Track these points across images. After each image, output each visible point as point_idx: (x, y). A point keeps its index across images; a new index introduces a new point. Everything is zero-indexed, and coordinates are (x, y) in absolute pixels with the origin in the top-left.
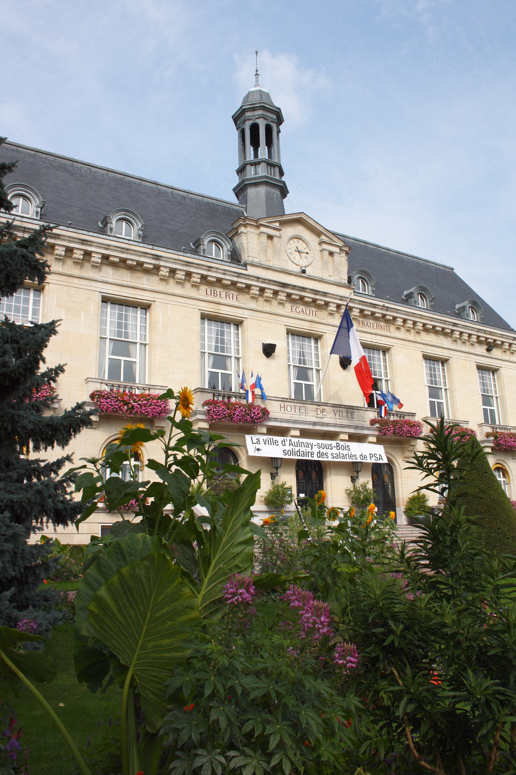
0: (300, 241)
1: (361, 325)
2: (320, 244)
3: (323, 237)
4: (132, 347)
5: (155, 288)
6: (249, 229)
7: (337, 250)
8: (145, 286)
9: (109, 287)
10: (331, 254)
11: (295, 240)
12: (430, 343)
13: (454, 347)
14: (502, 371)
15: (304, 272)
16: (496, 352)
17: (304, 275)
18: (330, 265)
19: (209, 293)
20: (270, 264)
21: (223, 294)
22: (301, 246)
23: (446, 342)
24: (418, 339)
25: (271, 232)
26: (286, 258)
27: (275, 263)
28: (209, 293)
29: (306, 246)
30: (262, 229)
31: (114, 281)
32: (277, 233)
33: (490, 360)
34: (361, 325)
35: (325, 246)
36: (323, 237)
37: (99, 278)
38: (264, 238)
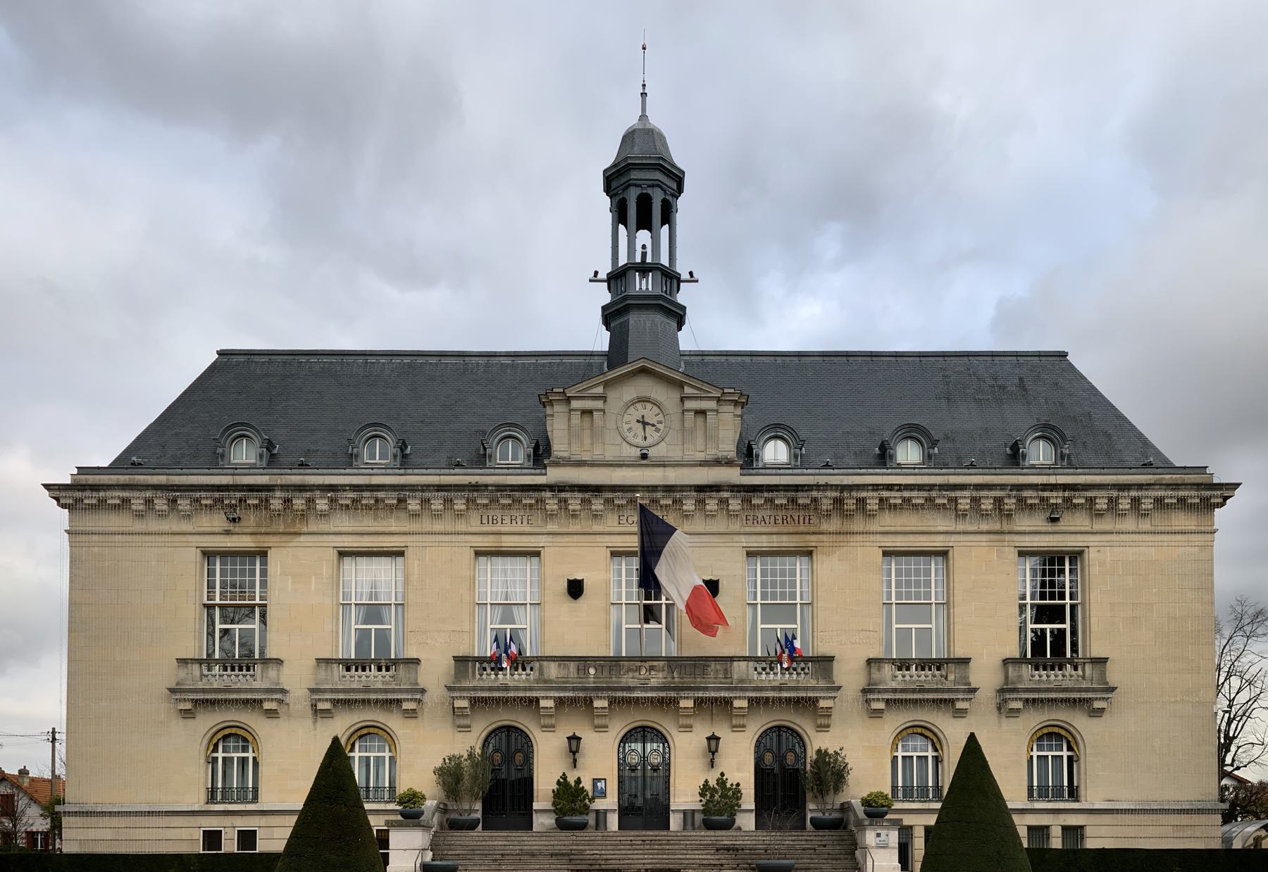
0: (649, 406)
1: (750, 523)
2: (682, 399)
3: (688, 390)
4: (384, 610)
5: (406, 529)
6: (558, 408)
7: (712, 404)
8: (393, 529)
9: (345, 538)
10: (702, 413)
11: (639, 406)
12: (899, 529)
13: (961, 527)
14: (1092, 556)
15: (644, 456)
17: (645, 462)
18: (700, 434)
19: (485, 521)
20: (586, 457)
21: (507, 520)
22: (650, 413)
23: (941, 522)
24: (874, 526)
27: (597, 453)
28: (485, 521)
29: (658, 411)
30: (575, 404)
31: (350, 530)
32: (599, 404)
33: (1057, 537)
34: (750, 523)
35: (689, 404)
36: (688, 390)
37: (333, 529)
38: (576, 418)
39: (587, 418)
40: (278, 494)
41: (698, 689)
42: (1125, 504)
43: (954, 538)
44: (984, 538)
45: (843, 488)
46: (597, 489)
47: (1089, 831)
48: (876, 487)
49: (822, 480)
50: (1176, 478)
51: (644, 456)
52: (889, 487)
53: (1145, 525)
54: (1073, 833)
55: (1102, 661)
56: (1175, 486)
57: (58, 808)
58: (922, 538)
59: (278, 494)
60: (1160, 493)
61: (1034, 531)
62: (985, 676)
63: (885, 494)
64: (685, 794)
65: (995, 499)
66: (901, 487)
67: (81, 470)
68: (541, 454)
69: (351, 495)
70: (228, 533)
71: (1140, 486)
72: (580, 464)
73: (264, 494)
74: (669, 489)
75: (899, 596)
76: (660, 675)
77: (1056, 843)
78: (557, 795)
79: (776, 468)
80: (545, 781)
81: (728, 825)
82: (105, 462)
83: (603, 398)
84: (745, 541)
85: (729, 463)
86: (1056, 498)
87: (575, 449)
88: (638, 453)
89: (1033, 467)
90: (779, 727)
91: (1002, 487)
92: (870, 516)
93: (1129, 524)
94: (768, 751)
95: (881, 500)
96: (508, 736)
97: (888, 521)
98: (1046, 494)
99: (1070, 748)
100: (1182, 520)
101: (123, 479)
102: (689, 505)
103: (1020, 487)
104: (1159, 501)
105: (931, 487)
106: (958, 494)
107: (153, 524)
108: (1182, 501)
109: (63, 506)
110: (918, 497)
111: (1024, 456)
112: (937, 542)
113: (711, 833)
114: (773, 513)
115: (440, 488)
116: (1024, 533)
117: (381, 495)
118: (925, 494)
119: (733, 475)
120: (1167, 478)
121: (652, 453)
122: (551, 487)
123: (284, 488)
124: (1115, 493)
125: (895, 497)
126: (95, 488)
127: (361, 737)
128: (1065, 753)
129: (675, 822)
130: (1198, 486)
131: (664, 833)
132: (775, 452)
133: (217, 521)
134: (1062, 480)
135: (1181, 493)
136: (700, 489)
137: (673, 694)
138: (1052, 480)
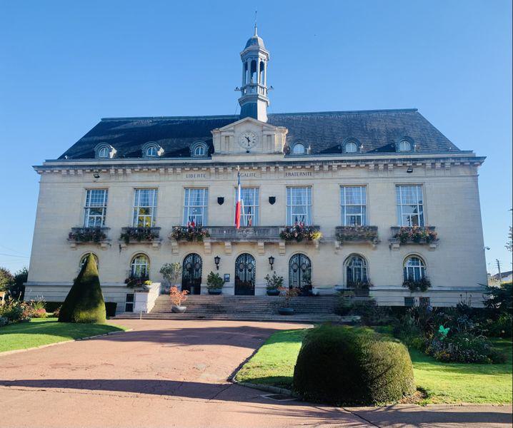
16: (418, 172)
24: (335, 176)
25: (228, 134)
26: (239, 146)
30: (223, 134)
32: (232, 134)
33: (412, 179)
35: (265, 133)
39: (227, 138)
40: (113, 168)
41: (265, 239)
42: (438, 165)
43: (370, 180)
44: (381, 179)
45: (323, 162)
46: (229, 164)
47: (431, 300)
48: (336, 161)
49: (316, 159)
50: (460, 155)
51: (248, 152)
52: (342, 161)
53: (448, 173)
54: (424, 300)
55: (432, 228)
56: (459, 158)
57: (24, 284)
58: (356, 180)
59: (113, 168)
60: (453, 161)
61: (401, 175)
62: (384, 233)
63: (339, 164)
64: (261, 283)
65: (385, 165)
66: (345, 161)
67: (47, 161)
68: (211, 151)
69: (139, 168)
70: (95, 182)
71: (444, 159)
72: (225, 155)
73: (108, 168)
74: (256, 164)
75: (347, 202)
76: (251, 233)
77: (417, 304)
78: (210, 281)
79: (298, 156)
80: (205, 274)
81: (277, 294)
82: (56, 158)
83: (233, 131)
84: (285, 182)
85: (280, 153)
86: (409, 164)
87: (223, 150)
88: (246, 150)
89: (401, 152)
90: (300, 254)
91: (387, 160)
92: (335, 171)
93: (442, 173)
94: (296, 263)
95: (338, 166)
96: (193, 258)
97: (342, 173)
98: (405, 162)
99: (422, 264)
100: (462, 171)
101: (60, 163)
102: (264, 169)
103: (394, 160)
104: (452, 164)
105: (358, 161)
106: (369, 163)
107: (68, 179)
108: (462, 164)
109: (39, 173)
110: (353, 165)
111: (398, 148)
112: (362, 182)
113: (270, 297)
114: (296, 171)
115: (172, 164)
116: (397, 177)
117: (150, 167)
118: (356, 163)
119: (282, 158)
120: (456, 155)
121: (251, 150)
122: (213, 164)
123: (115, 165)
124: (433, 161)
125: (344, 165)
126: (51, 167)
127: (138, 257)
128: (420, 266)
129: (257, 292)
130: (469, 158)
131: (253, 296)
132: (299, 149)
133: (91, 177)
134: (412, 156)
135: (462, 161)
136: (268, 163)
137: (255, 241)
138: (408, 157)
